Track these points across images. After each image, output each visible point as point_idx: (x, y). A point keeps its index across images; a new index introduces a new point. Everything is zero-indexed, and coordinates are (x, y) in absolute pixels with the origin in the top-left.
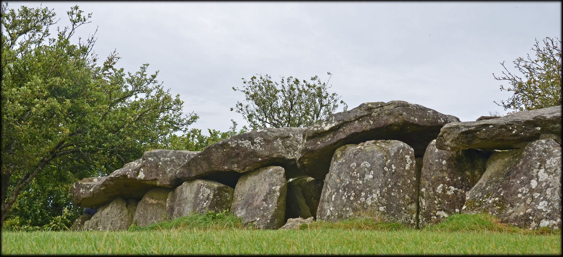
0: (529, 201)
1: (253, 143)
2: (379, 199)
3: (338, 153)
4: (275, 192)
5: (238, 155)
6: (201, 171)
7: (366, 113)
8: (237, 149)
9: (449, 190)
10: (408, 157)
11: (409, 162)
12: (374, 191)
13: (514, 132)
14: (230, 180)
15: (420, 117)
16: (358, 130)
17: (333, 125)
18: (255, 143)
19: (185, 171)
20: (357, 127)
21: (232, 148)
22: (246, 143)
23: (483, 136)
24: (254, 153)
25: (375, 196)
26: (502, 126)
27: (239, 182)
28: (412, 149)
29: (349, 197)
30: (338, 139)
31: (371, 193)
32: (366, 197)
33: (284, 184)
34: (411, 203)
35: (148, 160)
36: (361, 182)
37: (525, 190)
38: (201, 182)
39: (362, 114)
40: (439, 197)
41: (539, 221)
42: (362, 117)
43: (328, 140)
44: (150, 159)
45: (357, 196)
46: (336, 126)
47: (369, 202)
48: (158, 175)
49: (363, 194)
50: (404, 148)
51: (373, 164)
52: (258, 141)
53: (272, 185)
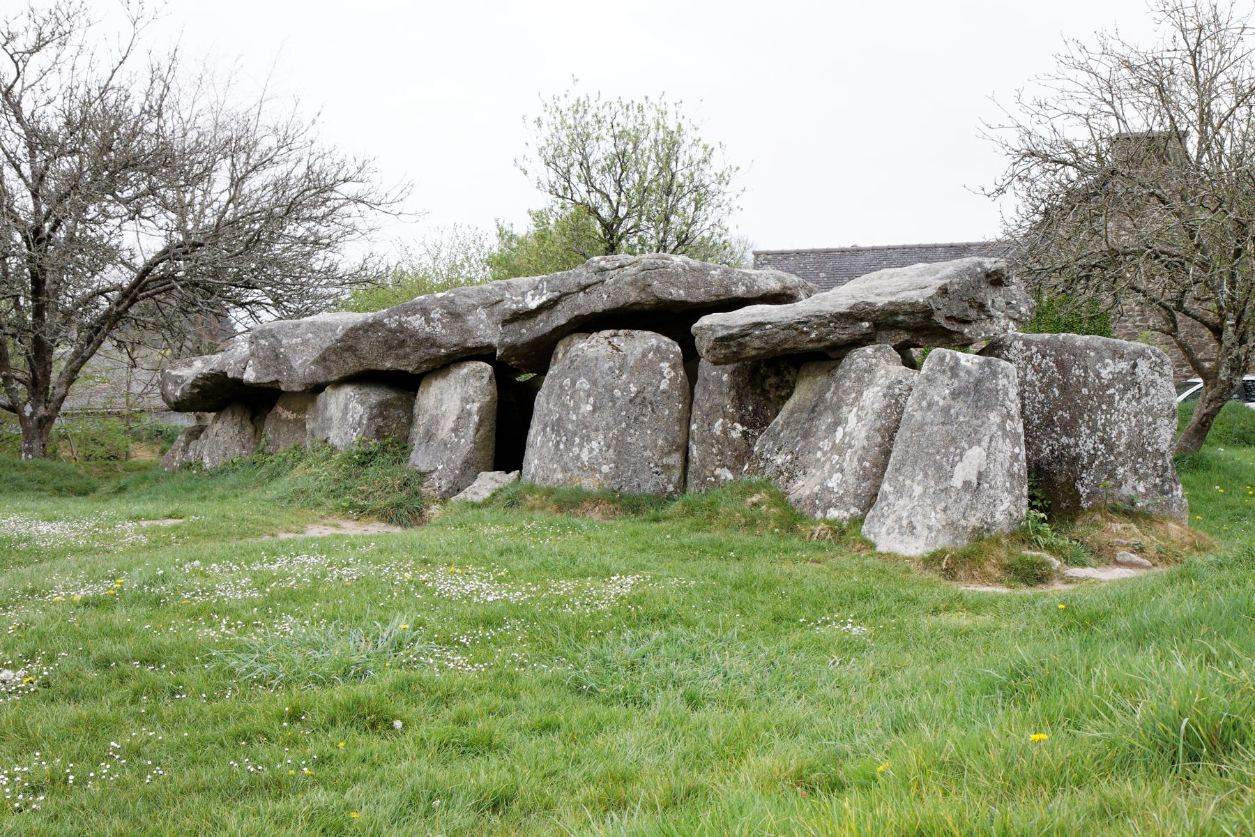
1: (428, 321)
2: (601, 450)
3: (560, 349)
4: (470, 414)
5: (402, 344)
7: (595, 278)
8: (401, 332)
9: (734, 429)
10: (665, 366)
11: (669, 373)
12: (593, 435)
13: (813, 335)
14: (406, 385)
15: (689, 287)
16: (584, 311)
17: (544, 299)
18: (433, 320)
21: (390, 330)
22: (416, 322)
23: (757, 344)
24: (430, 341)
25: (594, 444)
26: (789, 327)
27: (421, 389)
28: (678, 348)
29: (558, 442)
30: (555, 325)
31: (589, 440)
32: (581, 446)
33: (488, 399)
34: (669, 453)
35: (258, 344)
36: (574, 418)
39: (589, 281)
40: (718, 442)
42: (588, 286)
43: (542, 326)
44: (263, 342)
45: (569, 443)
46: (549, 301)
47: (585, 456)
48: (279, 372)
49: (577, 440)
50: (658, 350)
51: (594, 383)
52: (438, 316)
53: (466, 400)
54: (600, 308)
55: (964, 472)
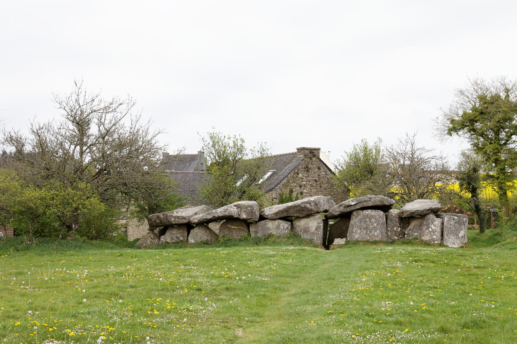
0: (429, 235)
1: (311, 205)
4: (320, 226)
6: (281, 216)
19: (275, 216)
20: (365, 204)
22: (308, 206)
24: (311, 210)
37: (427, 231)
38: (280, 221)
41: (434, 242)
43: (352, 208)
48: (252, 216)
51: (376, 220)
54: (370, 205)
55: (460, 235)
